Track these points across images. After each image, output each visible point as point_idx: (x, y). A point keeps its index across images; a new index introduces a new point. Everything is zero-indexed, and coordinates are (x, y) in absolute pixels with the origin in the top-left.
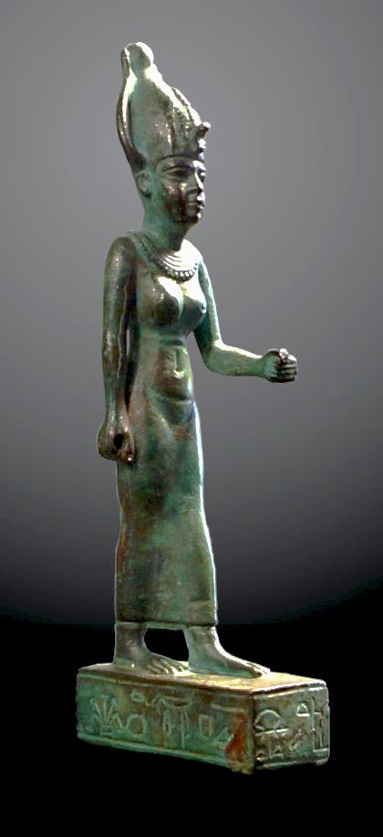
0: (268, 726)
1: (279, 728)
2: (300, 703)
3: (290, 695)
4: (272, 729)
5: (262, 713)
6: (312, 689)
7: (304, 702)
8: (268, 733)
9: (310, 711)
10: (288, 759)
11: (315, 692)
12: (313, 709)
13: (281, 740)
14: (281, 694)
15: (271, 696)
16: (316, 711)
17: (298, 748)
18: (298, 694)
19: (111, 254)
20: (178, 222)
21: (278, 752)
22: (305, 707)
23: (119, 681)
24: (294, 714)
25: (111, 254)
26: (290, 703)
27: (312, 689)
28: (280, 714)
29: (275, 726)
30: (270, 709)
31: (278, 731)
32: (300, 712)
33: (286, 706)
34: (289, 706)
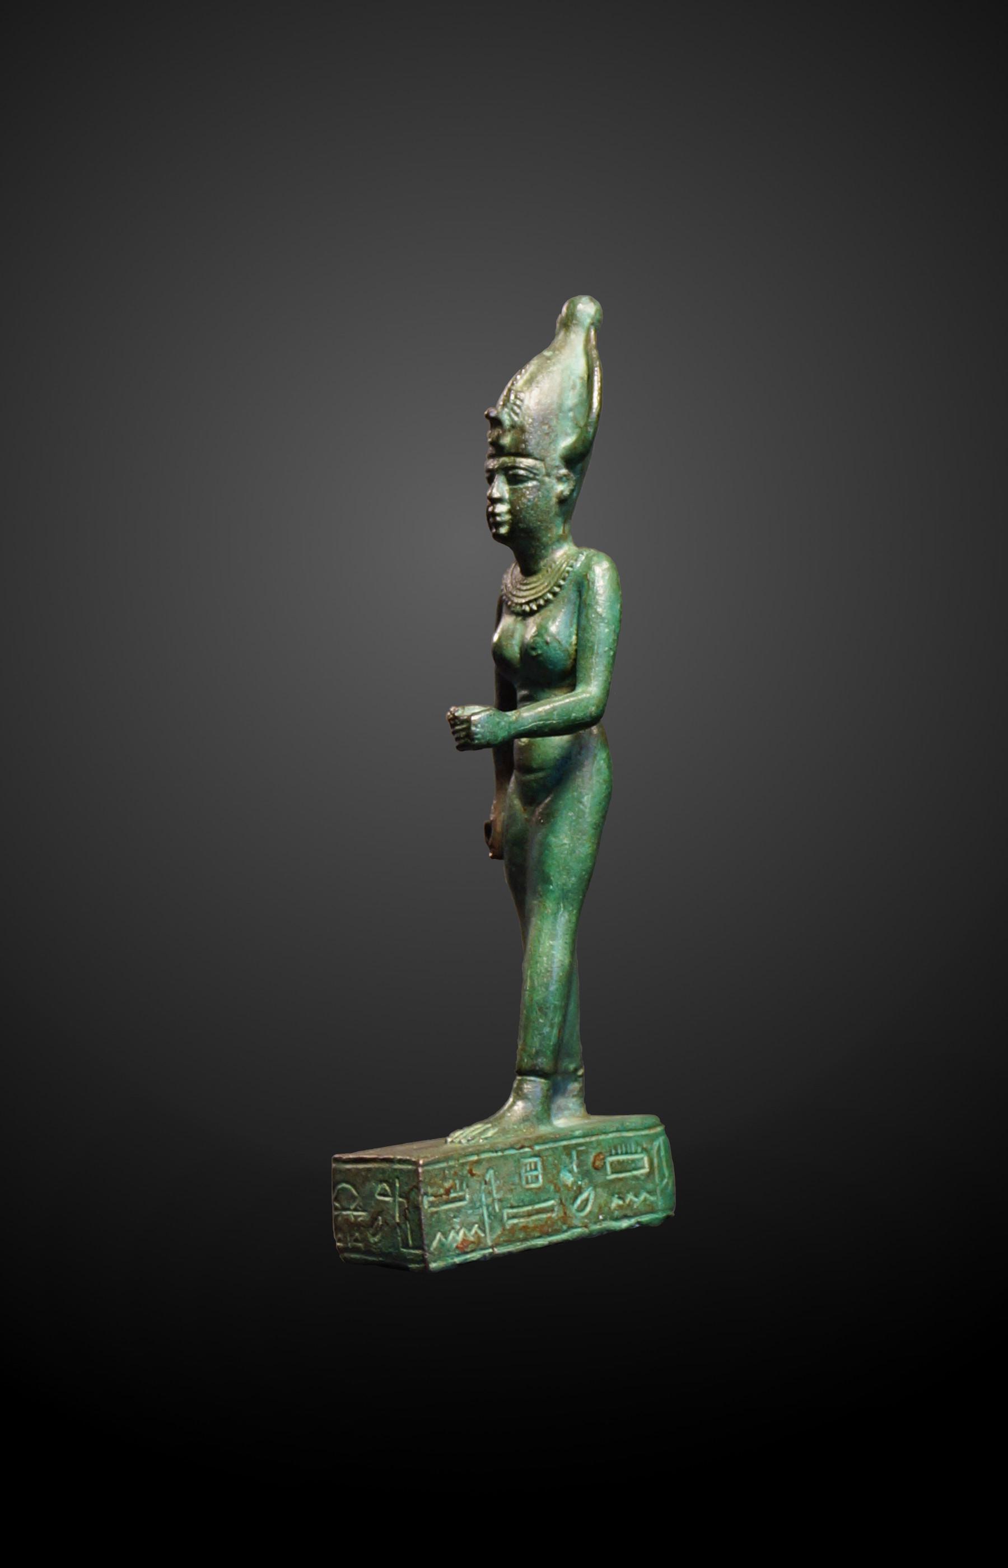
0: (345, 1204)
1: (356, 1210)
2: (381, 1181)
3: (369, 1170)
4: (349, 1209)
5: (340, 1186)
6: (398, 1166)
7: (386, 1181)
8: (344, 1213)
9: (393, 1196)
10: (368, 1252)
11: (401, 1170)
12: (528, 1165)
13: (356, 1225)
14: (361, 1166)
15: (348, 1166)
16: (401, 1196)
17: (380, 1241)
18: (378, 1169)
19: (577, 497)
20: (560, 395)
21: (356, 1240)
22: (387, 1188)
23: (544, 1050)
24: (372, 1195)
25: (577, 497)
26: (369, 1181)
27: (398, 1166)
28: (358, 1193)
29: (352, 1207)
30: (347, 1182)
31: (356, 1213)
32: (380, 1194)
33: (364, 1183)
34: (367, 1184)
